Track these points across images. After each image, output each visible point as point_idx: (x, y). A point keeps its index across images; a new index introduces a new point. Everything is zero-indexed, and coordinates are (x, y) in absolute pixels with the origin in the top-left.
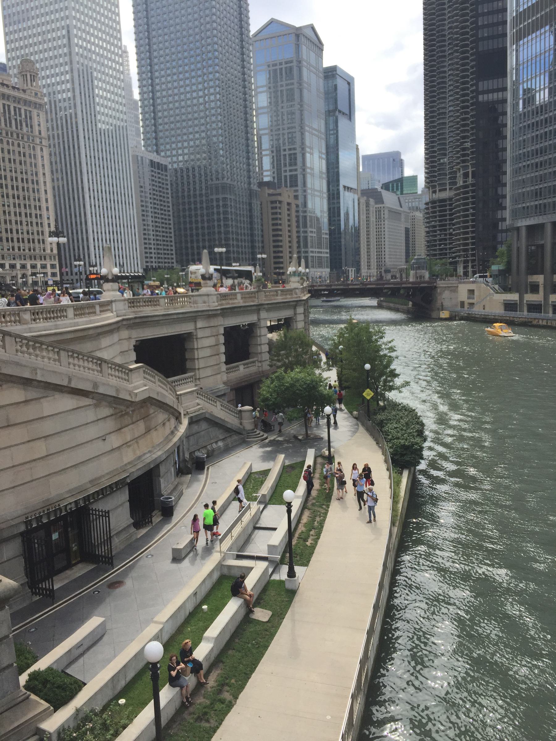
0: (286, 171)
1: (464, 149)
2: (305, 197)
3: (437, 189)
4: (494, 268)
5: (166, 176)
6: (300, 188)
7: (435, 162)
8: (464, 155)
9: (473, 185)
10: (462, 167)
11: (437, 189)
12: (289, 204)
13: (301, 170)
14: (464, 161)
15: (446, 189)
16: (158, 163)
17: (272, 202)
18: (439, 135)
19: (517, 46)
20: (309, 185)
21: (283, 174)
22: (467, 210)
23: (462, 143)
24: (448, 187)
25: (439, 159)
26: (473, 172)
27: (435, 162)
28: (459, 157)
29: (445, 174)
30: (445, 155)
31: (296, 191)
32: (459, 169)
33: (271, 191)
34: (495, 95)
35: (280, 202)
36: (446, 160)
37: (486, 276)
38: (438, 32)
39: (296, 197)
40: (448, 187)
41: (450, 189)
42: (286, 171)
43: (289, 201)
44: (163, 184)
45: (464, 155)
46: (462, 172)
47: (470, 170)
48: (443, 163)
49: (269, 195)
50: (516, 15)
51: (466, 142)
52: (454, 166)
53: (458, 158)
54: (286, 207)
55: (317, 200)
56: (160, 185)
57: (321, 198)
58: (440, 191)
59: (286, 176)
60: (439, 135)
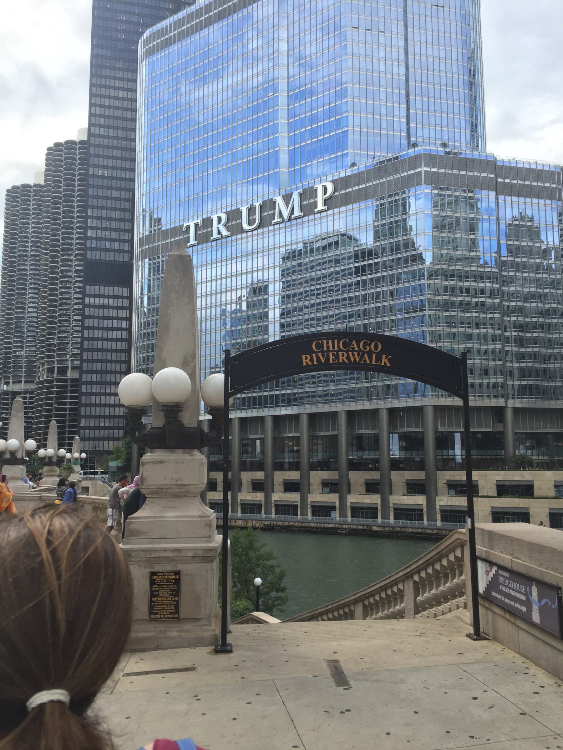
1: (50, 345)
3: (11, 381)
4: (113, 464)
7: (10, 353)
8: (49, 351)
9: (58, 381)
10: (47, 362)
11: (11, 381)
14: (49, 357)
15: (21, 382)
18: (16, 327)
19: (142, 262)
22: (51, 405)
23: (48, 339)
24: (23, 380)
25: (15, 351)
26: (58, 367)
27: (10, 353)
28: (43, 352)
29: (21, 367)
30: (22, 348)
32: (43, 364)
34: (97, 300)
36: (22, 353)
37: (96, 473)
38: (21, 232)
40: (23, 380)
41: (26, 382)
45: (49, 351)
46: (46, 367)
47: (56, 366)
48: (19, 356)
50: (143, 237)
51: (53, 339)
52: (38, 359)
53: (43, 352)
58: (14, 382)
60: (16, 327)
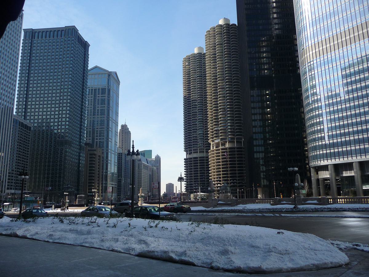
0: (97, 139)
2: (107, 154)
5: (30, 133)
6: (105, 148)
12: (99, 156)
13: (106, 139)
16: (26, 125)
17: (91, 154)
20: (110, 148)
21: (96, 140)
31: (103, 150)
33: (89, 148)
35: (95, 155)
39: (103, 153)
42: (97, 139)
43: (100, 155)
44: (27, 137)
49: (89, 150)
54: (98, 158)
55: (113, 155)
56: (25, 138)
57: (115, 155)
59: (97, 142)
